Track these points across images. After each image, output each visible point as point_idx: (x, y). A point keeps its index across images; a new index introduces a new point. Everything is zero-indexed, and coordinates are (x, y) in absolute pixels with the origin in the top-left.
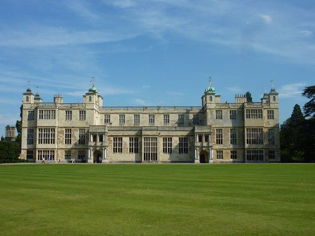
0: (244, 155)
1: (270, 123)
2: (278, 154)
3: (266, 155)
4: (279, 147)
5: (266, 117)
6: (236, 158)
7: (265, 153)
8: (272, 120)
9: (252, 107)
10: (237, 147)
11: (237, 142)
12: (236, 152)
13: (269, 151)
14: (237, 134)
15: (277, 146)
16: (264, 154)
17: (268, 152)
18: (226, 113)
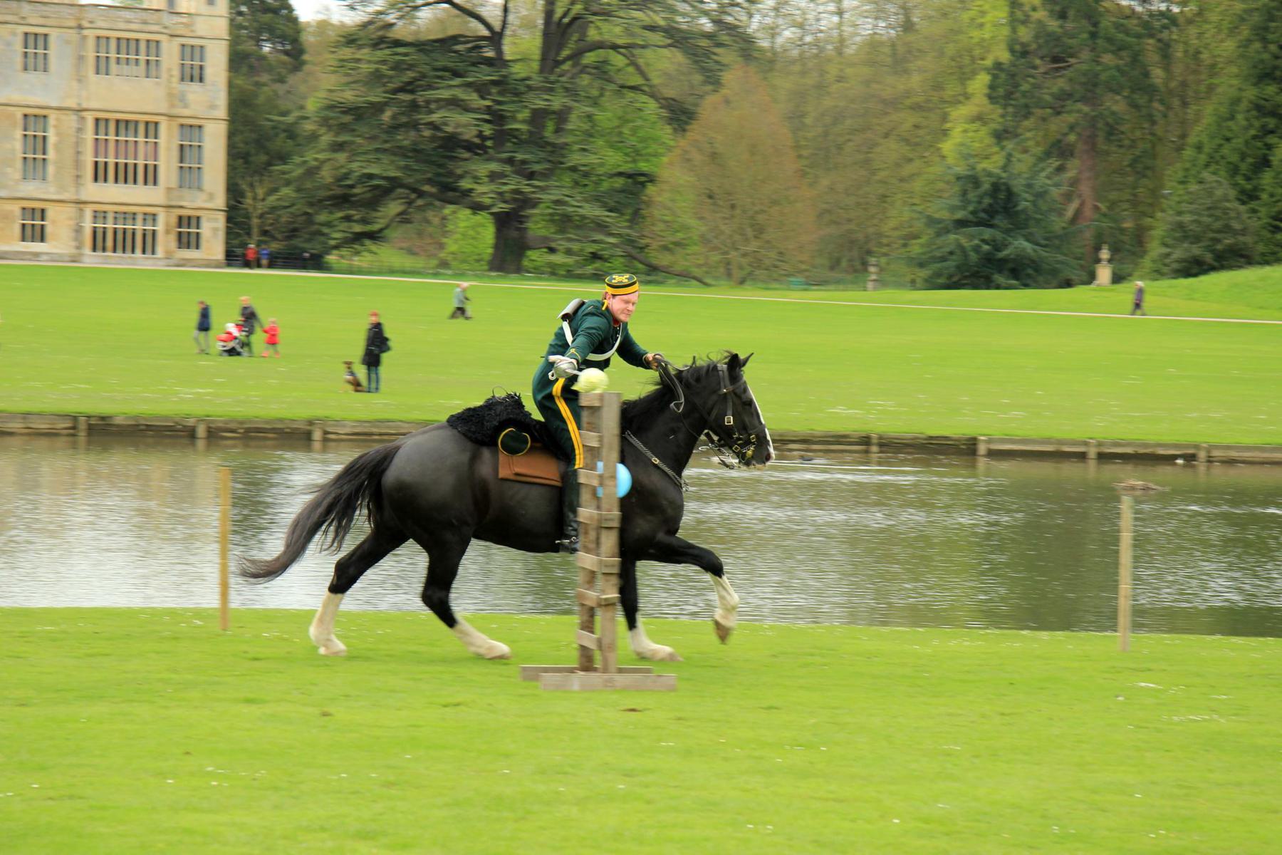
0: (78, 230)
1: (191, 97)
2: (215, 230)
3: (167, 232)
4: (220, 201)
5: (176, 73)
6: (42, 240)
7: (167, 224)
8: (195, 86)
9: (122, 26)
10: (50, 191)
11: (51, 169)
12: (43, 211)
13: (180, 218)
14: (52, 139)
15: (211, 197)
16: (160, 228)
17: (174, 221)
18: (8, 44)
